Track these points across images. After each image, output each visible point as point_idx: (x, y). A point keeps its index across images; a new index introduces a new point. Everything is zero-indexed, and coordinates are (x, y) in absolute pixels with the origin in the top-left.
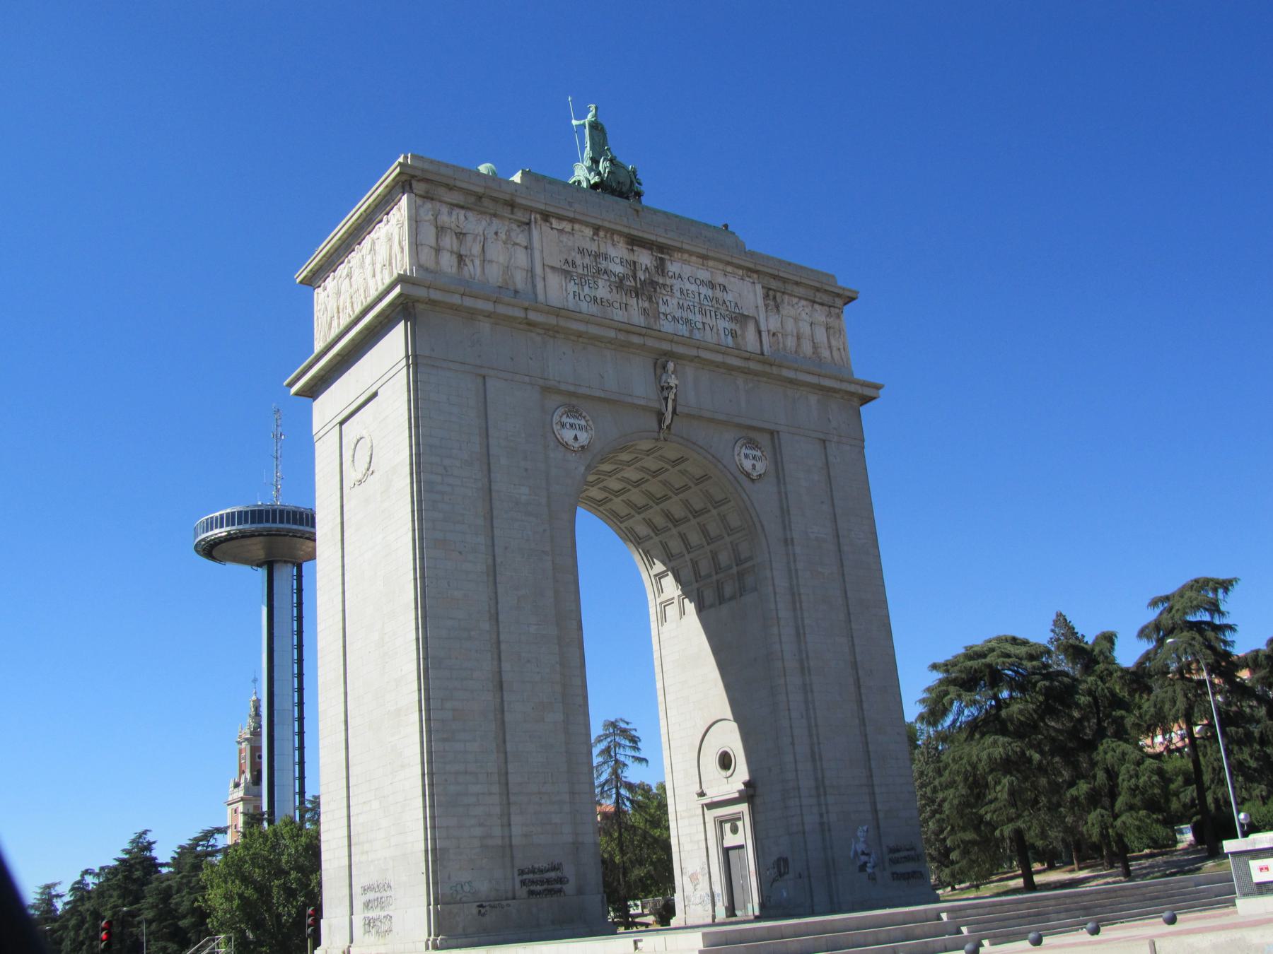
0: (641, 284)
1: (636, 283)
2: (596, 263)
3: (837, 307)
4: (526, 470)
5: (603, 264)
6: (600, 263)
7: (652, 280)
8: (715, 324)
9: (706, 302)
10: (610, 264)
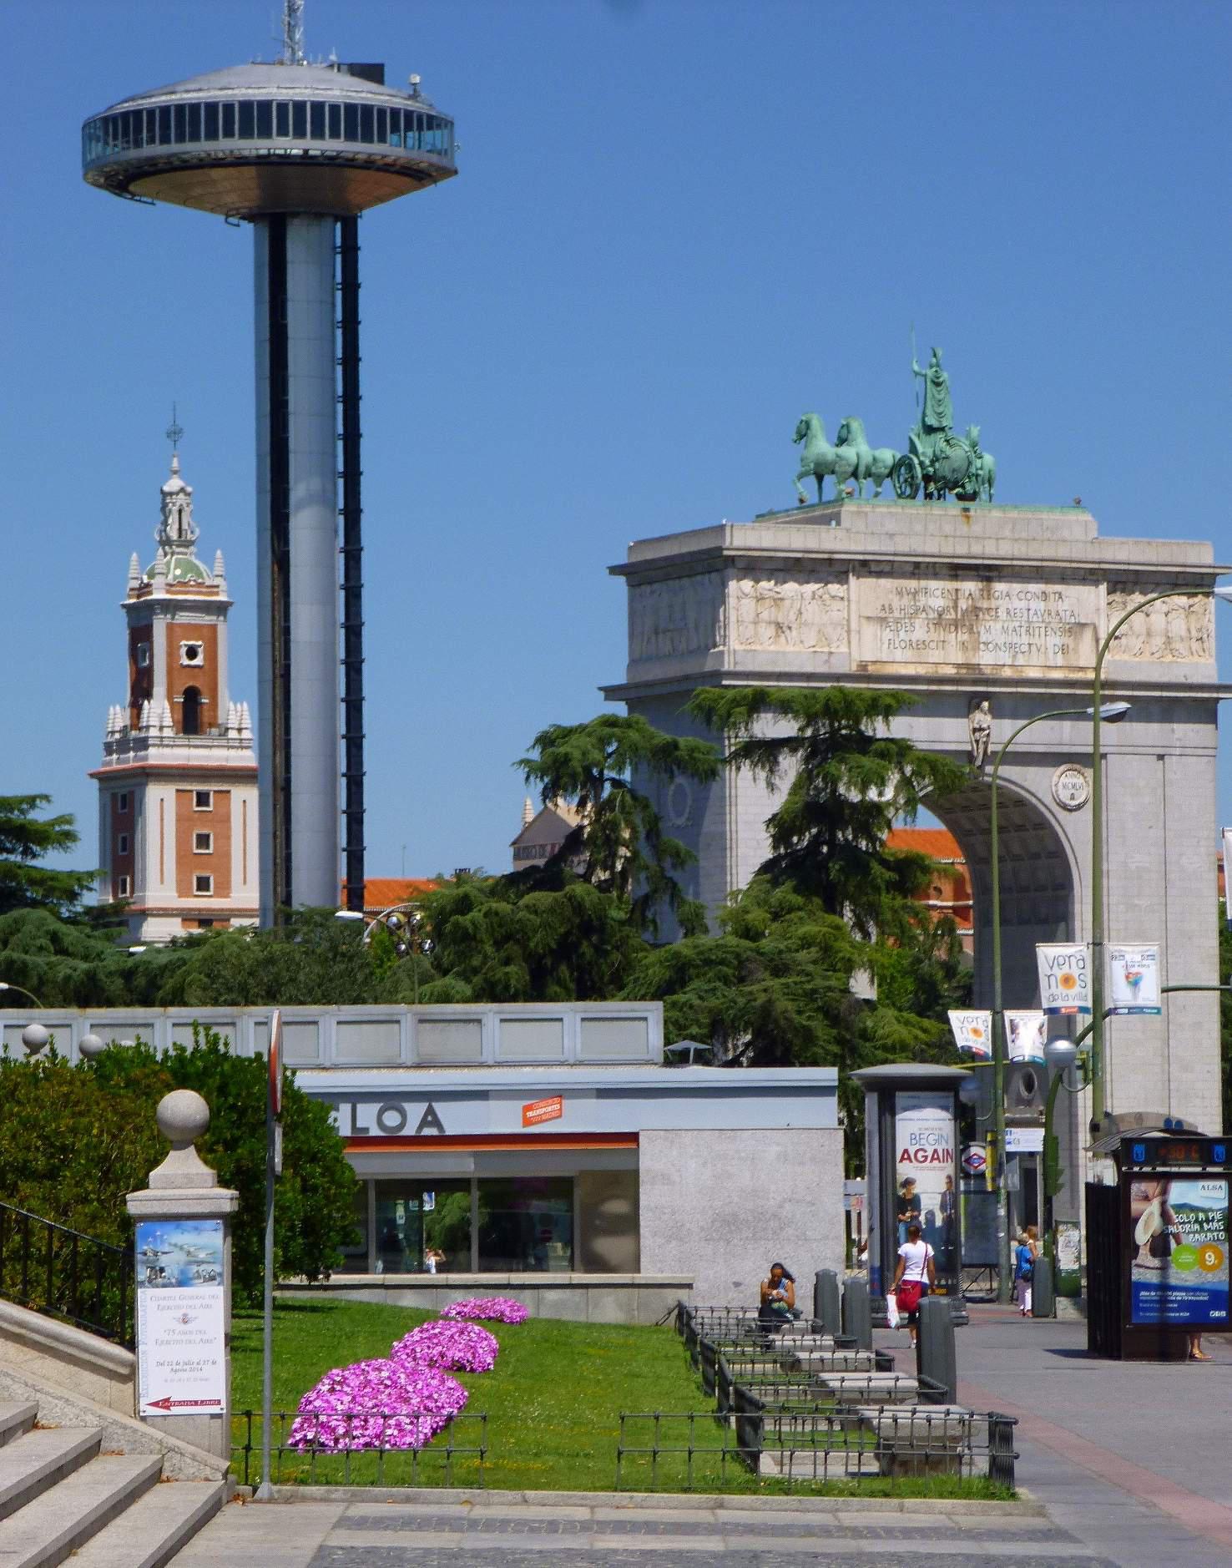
0: (963, 615)
5: (922, 601)
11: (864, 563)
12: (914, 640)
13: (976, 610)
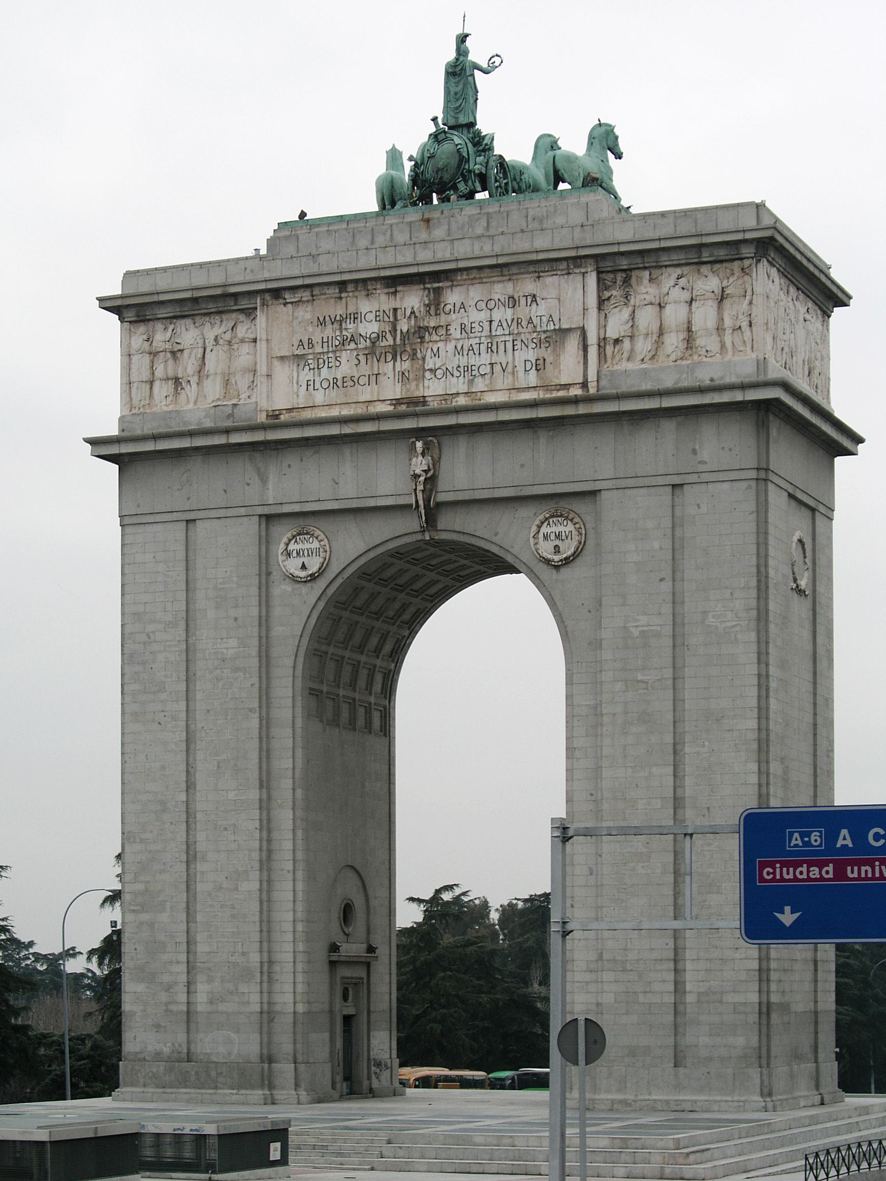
0: (403, 339)
1: (395, 340)
2: (341, 332)
3: (747, 258)
4: (236, 619)
6: (346, 329)
7: (420, 327)
8: (510, 359)
9: (500, 332)
10: (360, 324)
11: (277, 293)
12: (339, 377)
13: (421, 332)
